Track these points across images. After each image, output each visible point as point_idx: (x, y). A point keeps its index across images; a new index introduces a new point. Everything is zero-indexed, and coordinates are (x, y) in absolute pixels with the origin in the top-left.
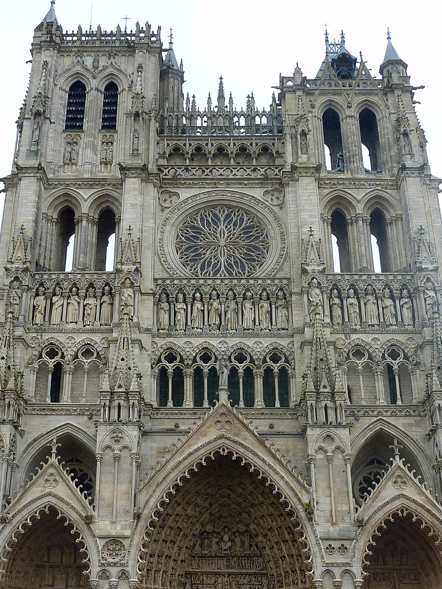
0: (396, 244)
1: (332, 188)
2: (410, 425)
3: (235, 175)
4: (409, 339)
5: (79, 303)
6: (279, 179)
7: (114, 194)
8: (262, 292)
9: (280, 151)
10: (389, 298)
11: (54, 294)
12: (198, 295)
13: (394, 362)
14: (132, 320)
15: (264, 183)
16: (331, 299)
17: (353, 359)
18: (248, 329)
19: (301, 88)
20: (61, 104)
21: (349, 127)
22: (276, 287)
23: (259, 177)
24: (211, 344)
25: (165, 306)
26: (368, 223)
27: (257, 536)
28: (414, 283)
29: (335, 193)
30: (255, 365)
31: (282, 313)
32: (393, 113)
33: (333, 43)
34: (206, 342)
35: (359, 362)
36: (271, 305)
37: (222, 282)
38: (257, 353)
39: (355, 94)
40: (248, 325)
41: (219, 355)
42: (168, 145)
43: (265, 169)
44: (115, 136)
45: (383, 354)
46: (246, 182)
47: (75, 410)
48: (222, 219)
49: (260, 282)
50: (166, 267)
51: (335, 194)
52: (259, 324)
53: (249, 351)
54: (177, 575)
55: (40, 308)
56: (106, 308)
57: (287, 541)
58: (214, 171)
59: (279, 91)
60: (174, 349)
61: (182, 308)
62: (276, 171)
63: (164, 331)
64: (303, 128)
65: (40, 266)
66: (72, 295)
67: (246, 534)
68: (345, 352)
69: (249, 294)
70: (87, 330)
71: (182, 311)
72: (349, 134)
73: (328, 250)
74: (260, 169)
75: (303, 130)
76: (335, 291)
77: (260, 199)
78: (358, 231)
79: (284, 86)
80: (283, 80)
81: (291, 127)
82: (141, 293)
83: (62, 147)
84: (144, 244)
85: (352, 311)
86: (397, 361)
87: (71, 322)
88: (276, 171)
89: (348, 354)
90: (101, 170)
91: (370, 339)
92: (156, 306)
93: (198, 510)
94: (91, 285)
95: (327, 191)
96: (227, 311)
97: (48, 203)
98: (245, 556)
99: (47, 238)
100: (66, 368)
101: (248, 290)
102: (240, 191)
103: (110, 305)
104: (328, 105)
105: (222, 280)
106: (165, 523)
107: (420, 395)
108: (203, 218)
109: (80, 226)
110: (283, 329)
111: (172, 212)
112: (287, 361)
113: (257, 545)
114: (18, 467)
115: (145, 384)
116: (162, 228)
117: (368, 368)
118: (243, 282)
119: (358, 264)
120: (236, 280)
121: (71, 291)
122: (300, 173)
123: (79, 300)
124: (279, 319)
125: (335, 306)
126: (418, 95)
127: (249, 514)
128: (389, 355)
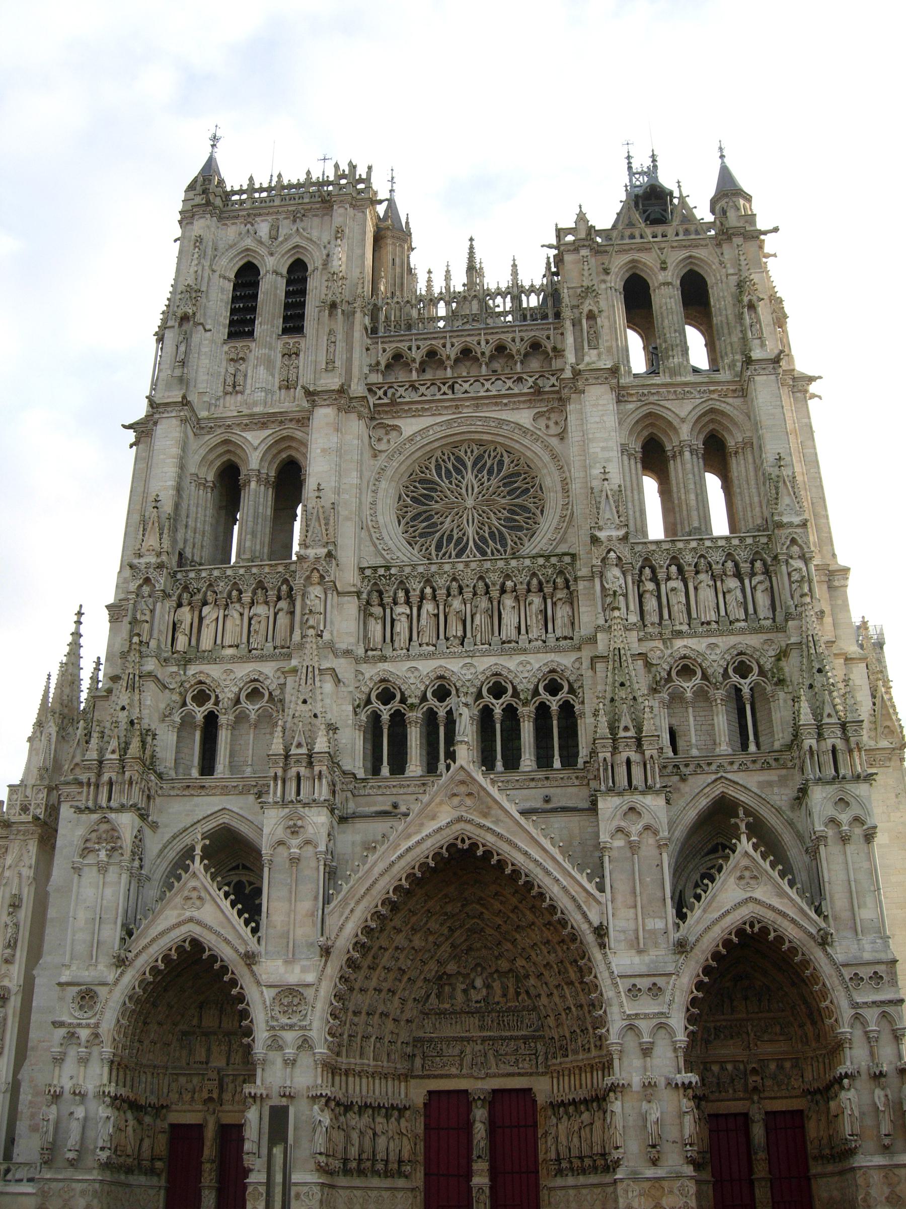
0: (745, 486)
1: (640, 400)
2: (770, 784)
4: (766, 641)
5: (242, 615)
6: (558, 392)
7: (299, 434)
8: (531, 579)
9: (559, 347)
10: (734, 576)
11: (205, 603)
12: (428, 590)
13: (742, 681)
14: (321, 636)
17: (678, 682)
19: (587, 243)
20: (222, 300)
21: (664, 300)
23: (526, 391)
24: (449, 670)
25: (377, 610)
26: (700, 455)
27: (527, 977)
28: (771, 549)
29: (645, 408)
30: (520, 699)
32: (732, 274)
33: (639, 170)
34: (441, 666)
35: (688, 685)
36: (545, 599)
38: (524, 681)
39: (673, 247)
41: (462, 686)
42: (384, 351)
44: (303, 345)
45: (726, 670)
46: (505, 401)
47: (235, 787)
48: (469, 464)
49: (527, 562)
50: (380, 547)
51: (645, 410)
52: (527, 633)
53: (510, 677)
54: (399, 1043)
55: (183, 626)
56: (283, 619)
57: (572, 983)
58: (456, 386)
59: (556, 252)
60: (390, 681)
62: (553, 380)
63: (374, 653)
64: (591, 308)
65: (187, 559)
66: (232, 603)
67: (510, 975)
69: (509, 584)
71: (404, 619)
72: (665, 314)
73: (637, 503)
74: (528, 378)
75: (590, 311)
76: (647, 571)
78: (683, 470)
79: (562, 242)
80: (560, 233)
81: (573, 307)
82: (338, 593)
83: (223, 367)
84: (343, 512)
85: (673, 601)
86: (748, 681)
87: (230, 646)
88: (553, 380)
89: (669, 674)
91: (704, 645)
92: (362, 613)
93: (431, 939)
94: (261, 585)
95: (631, 406)
96: (475, 614)
97: (198, 458)
98: (509, 1010)
99: (197, 513)
100: (223, 719)
101: (508, 577)
103: (289, 616)
104: (631, 268)
105: (467, 564)
106: (377, 961)
107: (786, 733)
110: (565, 638)
111: (390, 458)
112: (572, 691)
113: (527, 992)
114: (148, 879)
115: (344, 741)
117: (701, 694)
118: (501, 564)
119: (686, 522)
120: (489, 562)
121: (229, 595)
122: (587, 379)
123: (241, 610)
124: (558, 622)
125: (647, 595)
126: (770, 243)
127: (514, 942)
128: (735, 671)
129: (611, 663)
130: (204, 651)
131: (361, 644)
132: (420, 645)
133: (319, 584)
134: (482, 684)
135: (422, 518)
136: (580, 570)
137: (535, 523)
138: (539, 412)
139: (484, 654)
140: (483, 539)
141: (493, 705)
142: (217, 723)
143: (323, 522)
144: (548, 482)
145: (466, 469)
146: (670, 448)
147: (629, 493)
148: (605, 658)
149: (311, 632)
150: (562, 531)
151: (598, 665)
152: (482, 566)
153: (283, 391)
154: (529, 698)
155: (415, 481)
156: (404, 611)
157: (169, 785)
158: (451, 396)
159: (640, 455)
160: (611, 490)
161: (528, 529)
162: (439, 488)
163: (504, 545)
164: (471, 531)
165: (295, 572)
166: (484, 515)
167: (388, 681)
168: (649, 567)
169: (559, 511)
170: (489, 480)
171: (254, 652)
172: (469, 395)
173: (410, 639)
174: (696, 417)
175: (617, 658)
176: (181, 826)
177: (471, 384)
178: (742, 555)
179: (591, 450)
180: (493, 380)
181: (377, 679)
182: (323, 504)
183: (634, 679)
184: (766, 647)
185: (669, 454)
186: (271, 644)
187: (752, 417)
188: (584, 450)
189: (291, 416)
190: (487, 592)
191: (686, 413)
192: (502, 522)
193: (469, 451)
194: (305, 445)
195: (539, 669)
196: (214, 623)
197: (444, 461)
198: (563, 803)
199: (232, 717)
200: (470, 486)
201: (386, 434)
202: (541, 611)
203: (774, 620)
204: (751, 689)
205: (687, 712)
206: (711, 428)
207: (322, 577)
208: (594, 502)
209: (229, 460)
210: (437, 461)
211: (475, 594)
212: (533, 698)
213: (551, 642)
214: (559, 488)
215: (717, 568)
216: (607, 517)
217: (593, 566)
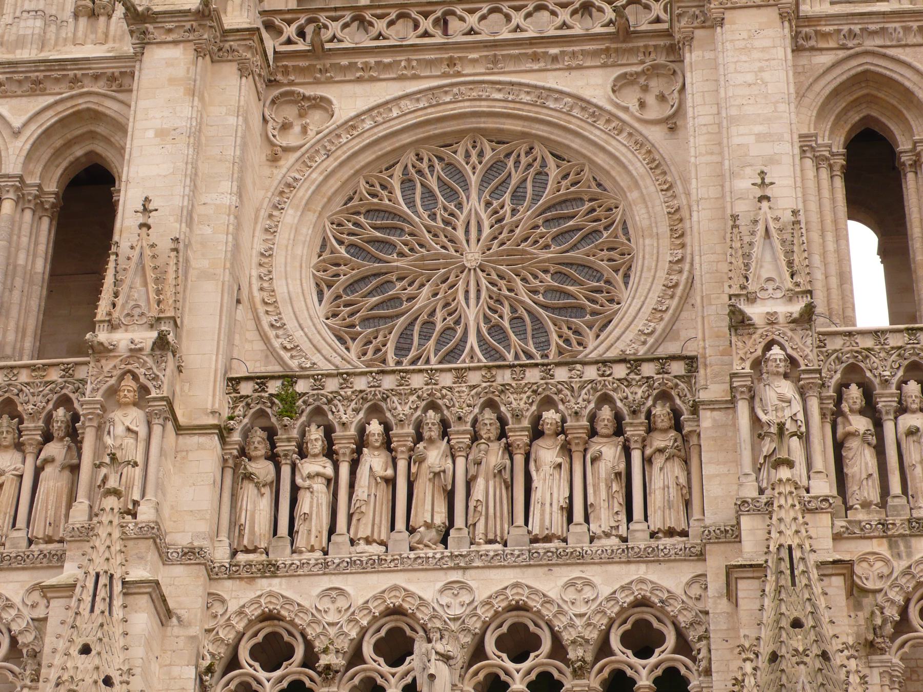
3: (518, 28)
6: (668, 34)
7: (110, 107)
8: (599, 406)
12: (375, 427)
14: (134, 516)
15: (617, 50)
16: (840, 420)
18: (548, 539)
22: (644, 388)
23: (599, 30)
25: (263, 469)
30: (567, 662)
34: (395, 588)
38: (578, 622)
40: (547, 523)
46: (554, 51)
49: (591, 373)
51: (854, 67)
52: (587, 520)
53: (548, 613)
61: (318, 475)
63: (251, 557)
68: (892, 602)
69: (550, 416)
71: (319, 486)
73: (832, 258)
76: (854, 392)
77: (600, 103)
82: (179, 429)
84: (198, 263)
90: (74, 34)
92: (229, 473)
95: (825, 59)
96: (475, 478)
101: (548, 403)
103: (67, 473)
105: (460, 375)
108: (410, 180)
110: (671, 533)
111: (306, 162)
112: (684, 646)
120: (508, 373)
124: (657, 499)
129: (771, 578)
131: (224, 537)
132: (352, 542)
133: (135, 404)
135: (370, 286)
137: (611, 301)
138: (626, 74)
140: (496, 330)
141: (507, 673)
143: (151, 275)
144: (640, 217)
145: (466, 188)
146: (909, 146)
147: (815, 236)
148: (757, 570)
149: (111, 502)
150: (667, 317)
151: (742, 585)
152: (492, 379)
153: (83, 21)
154: (589, 658)
155: (358, 213)
156: (321, 470)
158: (439, 39)
159: (841, 161)
160: (777, 219)
161: (594, 313)
163: (543, 346)
164: (472, 314)
165: (83, 382)
166: (502, 283)
167: (279, 618)
168: (860, 385)
169: (662, 274)
170: (514, 211)
173: (332, 530)
175: (785, 566)
177: (483, 18)
179: (736, 140)
181: (253, 612)
182: (153, 239)
183: (825, 616)
185: (904, 158)
186: (22, 534)
188: (719, 143)
189: (97, 68)
190: (502, 435)
192: (541, 298)
193: (474, 153)
194: (121, 128)
195: (611, 598)
197: (420, 172)
200: (473, 223)
201: (301, 116)
202: (618, 475)
207: (144, 390)
208: (737, 245)
211: (475, 438)
212: (597, 660)
213: (640, 541)
216: (765, 274)
217: (733, 375)
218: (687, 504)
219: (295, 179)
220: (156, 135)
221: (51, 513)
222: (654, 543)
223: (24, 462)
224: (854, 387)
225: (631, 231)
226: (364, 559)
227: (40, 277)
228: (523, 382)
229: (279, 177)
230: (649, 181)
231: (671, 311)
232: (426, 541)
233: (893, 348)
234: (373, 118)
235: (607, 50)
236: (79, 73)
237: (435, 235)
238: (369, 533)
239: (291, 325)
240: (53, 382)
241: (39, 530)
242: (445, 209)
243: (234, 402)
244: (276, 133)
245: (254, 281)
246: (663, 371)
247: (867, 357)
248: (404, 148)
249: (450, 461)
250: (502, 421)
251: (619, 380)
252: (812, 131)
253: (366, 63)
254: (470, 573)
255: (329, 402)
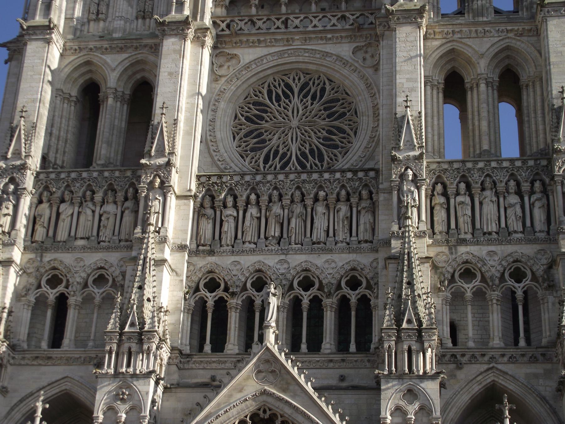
2: (536, 376)
5: (93, 212)
8: (341, 190)
10: (516, 193)
11: (63, 201)
13: (516, 285)
17: (460, 283)
23: (347, 27)
25: (210, 212)
26: (495, 87)
30: (324, 292)
31: (366, 218)
35: (468, 286)
36: (351, 208)
37: (287, 177)
40: (319, 237)
43: (355, 17)
45: (503, 274)
46: (329, 36)
47: (78, 358)
48: (296, 90)
49: (338, 175)
52: (334, 236)
55: (42, 220)
61: (231, 215)
63: (204, 248)
65: (50, 162)
66: (86, 201)
68: (449, 272)
69: (322, 194)
70: (100, 249)
71: (232, 220)
77: (347, 59)
78: (478, 99)
86: (522, 285)
87: (82, 238)
96: (292, 217)
99: (61, 123)
100: (72, 301)
101: (321, 188)
102: (320, 49)
103: (133, 214)
109: (105, 105)
110: (366, 241)
112: (369, 287)
116: (214, 105)
117: (479, 294)
119: (477, 146)
121: (84, 196)
123: (93, 208)
124: (361, 228)
128: (511, 275)
130: (59, 242)
134: (294, 277)
136: (382, 183)
137: (349, 142)
139: (296, 252)
140: (304, 155)
141: (301, 296)
142: (66, 303)
145: (293, 94)
153: (140, 21)
155: (249, 103)
156: (231, 213)
157: (20, 356)
159: (442, 86)
161: (342, 147)
162: (268, 109)
164: (294, 148)
166: (306, 134)
169: (369, 132)
170: (312, 104)
171: (102, 243)
172: (299, 30)
173: (236, 237)
174: (494, 53)
176: (29, 391)
178: (523, 175)
179: (398, 81)
180: (320, 17)
184: (539, 256)
187: (543, 54)
190: (303, 200)
191: (485, 50)
192: (321, 141)
193: (297, 78)
196: (69, 218)
197: (275, 86)
198: (356, 382)
199: (80, 299)
202: (347, 218)
203: (548, 233)
204: (525, 292)
205: (467, 309)
206: (506, 63)
209: (91, 79)
210: (269, 86)
211: (292, 201)
214: (371, 113)
215: (501, 187)
218: (373, 230)
219: (225, 89)
220: (168, 75)
221: (127, 230)
222: (359, 246)
223: (117, 209)
224: (439, 184)
225: (358, 113)
226: (248, 250)
227: (123, 129)
228: (311, 179)
229: (218, 88)
230: (365, 93)
231: (372, 148)
232: (272, 243)
233: (455, 169)
234: (255, 64)
235: (351, 35)
236: (138, 44)
237: (280, 113)
238: (250, 239)
239: (222, 150)
240: (128, 177)
241: (123, 237)
242: (285, 102)
243: (199, 185)
244: (217, 69)
245: (208, 132)
246: (366, 175)
247: (445, 172)
248: (268, 75)
249: (282, 211)
250: (303, 195)
251: (349, 179)
252: (431, 74)
253: (253, 40)
254: (289, 256)
255: (236, 186)
